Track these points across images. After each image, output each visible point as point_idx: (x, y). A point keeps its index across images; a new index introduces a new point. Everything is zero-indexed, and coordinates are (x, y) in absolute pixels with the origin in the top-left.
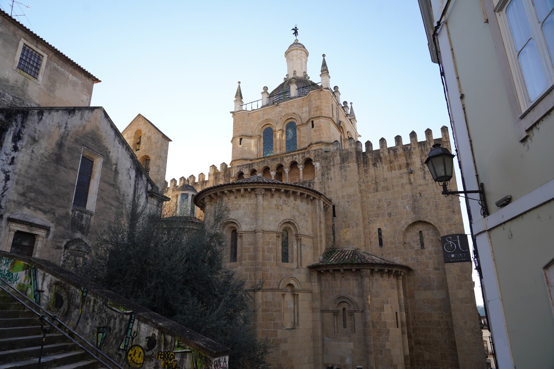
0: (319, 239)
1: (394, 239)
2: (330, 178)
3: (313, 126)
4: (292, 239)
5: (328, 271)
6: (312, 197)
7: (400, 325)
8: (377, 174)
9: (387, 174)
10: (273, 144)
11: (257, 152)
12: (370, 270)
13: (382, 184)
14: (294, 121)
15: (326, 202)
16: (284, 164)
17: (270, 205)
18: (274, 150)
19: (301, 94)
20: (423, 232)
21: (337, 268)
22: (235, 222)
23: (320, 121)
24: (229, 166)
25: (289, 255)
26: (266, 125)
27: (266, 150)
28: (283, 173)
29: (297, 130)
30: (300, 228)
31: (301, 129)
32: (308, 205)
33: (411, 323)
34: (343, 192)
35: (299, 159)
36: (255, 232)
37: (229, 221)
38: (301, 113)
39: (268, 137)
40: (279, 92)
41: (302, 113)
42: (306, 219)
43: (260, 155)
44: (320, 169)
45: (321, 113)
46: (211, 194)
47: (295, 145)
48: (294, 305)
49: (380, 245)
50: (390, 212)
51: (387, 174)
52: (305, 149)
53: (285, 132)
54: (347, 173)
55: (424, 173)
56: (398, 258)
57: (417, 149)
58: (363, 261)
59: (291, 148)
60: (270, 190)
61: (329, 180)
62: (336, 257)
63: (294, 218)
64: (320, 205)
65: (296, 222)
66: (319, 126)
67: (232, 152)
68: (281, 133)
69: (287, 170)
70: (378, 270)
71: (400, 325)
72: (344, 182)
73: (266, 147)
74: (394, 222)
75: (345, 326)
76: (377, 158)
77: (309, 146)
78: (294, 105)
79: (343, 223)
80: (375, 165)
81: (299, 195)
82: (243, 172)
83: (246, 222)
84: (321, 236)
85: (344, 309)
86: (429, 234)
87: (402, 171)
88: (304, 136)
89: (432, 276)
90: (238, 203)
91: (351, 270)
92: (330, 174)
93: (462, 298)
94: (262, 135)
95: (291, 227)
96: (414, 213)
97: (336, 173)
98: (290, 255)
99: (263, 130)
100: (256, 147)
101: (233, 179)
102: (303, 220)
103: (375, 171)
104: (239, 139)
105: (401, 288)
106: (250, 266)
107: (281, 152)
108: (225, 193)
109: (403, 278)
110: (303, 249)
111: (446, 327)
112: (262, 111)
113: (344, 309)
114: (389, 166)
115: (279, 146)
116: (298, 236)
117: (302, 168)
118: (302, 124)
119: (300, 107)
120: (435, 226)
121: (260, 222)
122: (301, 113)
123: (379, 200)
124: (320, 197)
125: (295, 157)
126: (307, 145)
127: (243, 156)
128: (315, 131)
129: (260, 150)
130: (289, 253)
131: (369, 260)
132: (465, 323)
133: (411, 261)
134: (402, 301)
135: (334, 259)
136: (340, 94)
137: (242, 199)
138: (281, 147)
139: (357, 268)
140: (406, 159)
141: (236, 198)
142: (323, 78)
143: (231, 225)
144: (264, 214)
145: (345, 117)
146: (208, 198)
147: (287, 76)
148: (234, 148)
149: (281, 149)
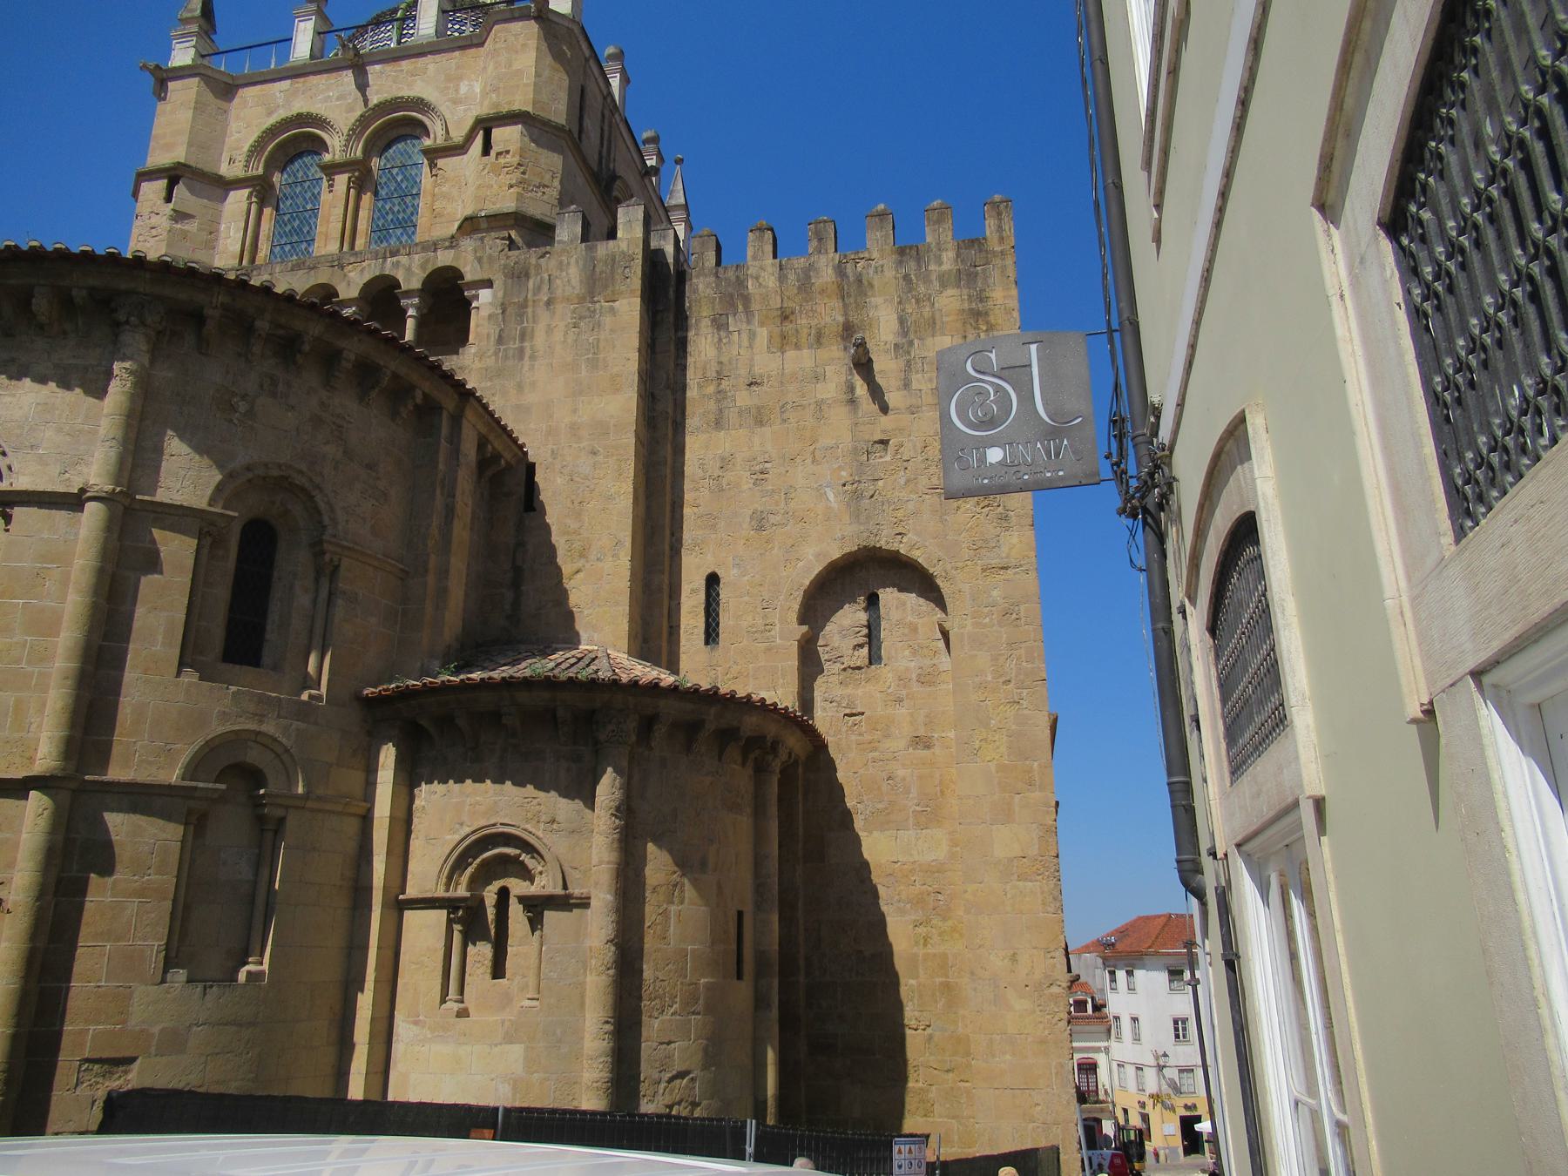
0: (431, 579)
2: (528, 352)
4: (293, 563)
7: (748, 967)
8: (724, 359)
9: (766, 362)
13: (744, 398)
15: (491, 438)
25: (268, 636)
33: (802, 963)
34: (575, 411)
35: (410, 273)
38: (449, 100)
44: (490, 316)
48: (257, 867)
49: (707, 643)
51: (766, 362)
54: (602, 337)
55: (908, 364)
57: (890, 273)
60: (196, 318)
61: (526, 358)
65: (318, 487)
66: (512, 148)
71: (748, 967)
72: (584, 373)
74: (772, 548)
75: (498, 970)
76: (731, 296)
80: (719, 324)
81: (349, 366)
83: (40, 451)
84: (444, 573)
85: (504, 894)
86: (904, 604)
87: (823, 354)
89: (901, 773)
90: (13, 360)
92: (532, 338)
93: (1011, 860)
96: (856, 515)
97: (558, 336)
98: (271, 635)
103: (719, 349)
104: (166, 181)
105: (773, 810)
106: (29, 662)
111: (938, 980)
113: (504, 894)
114: (777, 330)
123: (723, 459)
125: (395, 259)
127: (173, 252)
128: (496, 170)
130: (268, 628)
132: (1014, 958)
133: (824, 709)
134: (773, 866)
140: (845, 306)
145: (638, 178)
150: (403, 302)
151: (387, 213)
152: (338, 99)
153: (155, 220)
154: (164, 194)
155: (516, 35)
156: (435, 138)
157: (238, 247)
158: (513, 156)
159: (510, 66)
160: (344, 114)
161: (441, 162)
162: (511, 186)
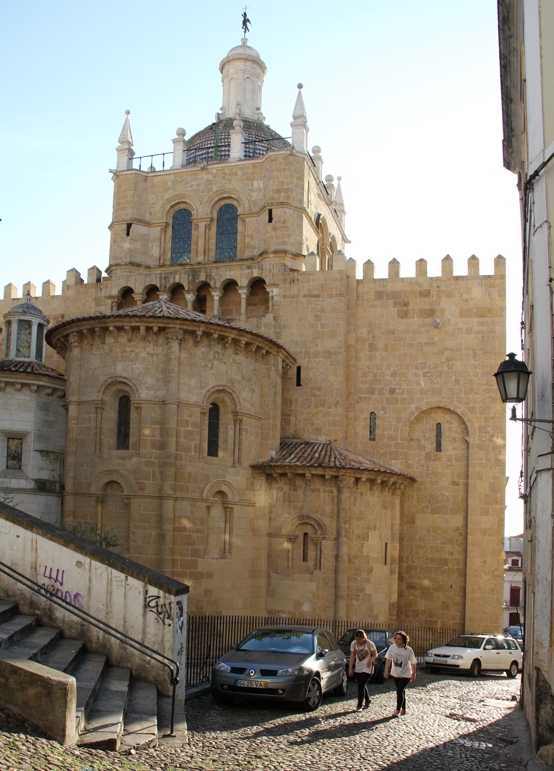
1: (394, 431)
3: (270, 220)
5: (284, 475)
6: (265, 350)
10: (191, 241)
11: (160, 253)
12: (354, 479)
14: (235, 203)
16: (212, 284)
17: (191, 358)
18: (193, 253)
19: (249, 152)
20: (442, 426)
21: (300, 472)
22: (128, 383)
23: (285, 212)
24: (104, 275)
26: (179, 203)
28: (208, 298)
29: (239, 222)
30: (242, 400)
31: (247, 220)
32: (257, 364)
36: (163, 403)
37: (116, 381)
38: (249, 190)
39: (181, 227)
40: (208, 140)
41: (252, 191)
42: (253, 387)
43: (164, 260)
45: (288, 197)
46: (82, 330)
47: (234, 249)
50: (393, 387)
52: (252, 259)
53: (215, 222)
56: (397, 461)
58: (343, 464)
59: (226, 253)
62: (298, 453)
63: (232, 383)
64: (278, 365)
67: (111, 247)
68: (209, 223)
69: (216, 295)
70: (367, 479)
77: (261, 255)
78: (236, 174)
79: (313, 399)
82: (133, 287)
88: (252, 235)
91: (323, 476)
94: (171, 221)
95: (227, 399)
99: (172, 212)
100: (159, 244)
101: (113, 300)
102: (246, 389)
107: (206, 258)
108: (109, 330)
109: (402, 493)
110: (243, 437)
115: (203, 247)
116: (238, 415)
117: (246, 293)
118: (251, 214)
119: (248, 179)
120: (463, 417)
121: (173, 386)
122: (249, 190)
124: (278, 352)
126: (256, 253)
128: (274, 229)
129: (164, 250)
131: (352, 462)
135: (295, 457)
136: (322, 163)
137: (141, 345)
139: (334, 474)
141: (130, 341)
142: (296, 131)
143: (120, 387)
144: (181, 373)
146: (75, 335)
147: (221, 109)
148: (114, 242)
149: (207, 254)
150: (240, 291)
151: (223, 241)
157: (158, 255)
158: (283, 223)
159: (278, 179)
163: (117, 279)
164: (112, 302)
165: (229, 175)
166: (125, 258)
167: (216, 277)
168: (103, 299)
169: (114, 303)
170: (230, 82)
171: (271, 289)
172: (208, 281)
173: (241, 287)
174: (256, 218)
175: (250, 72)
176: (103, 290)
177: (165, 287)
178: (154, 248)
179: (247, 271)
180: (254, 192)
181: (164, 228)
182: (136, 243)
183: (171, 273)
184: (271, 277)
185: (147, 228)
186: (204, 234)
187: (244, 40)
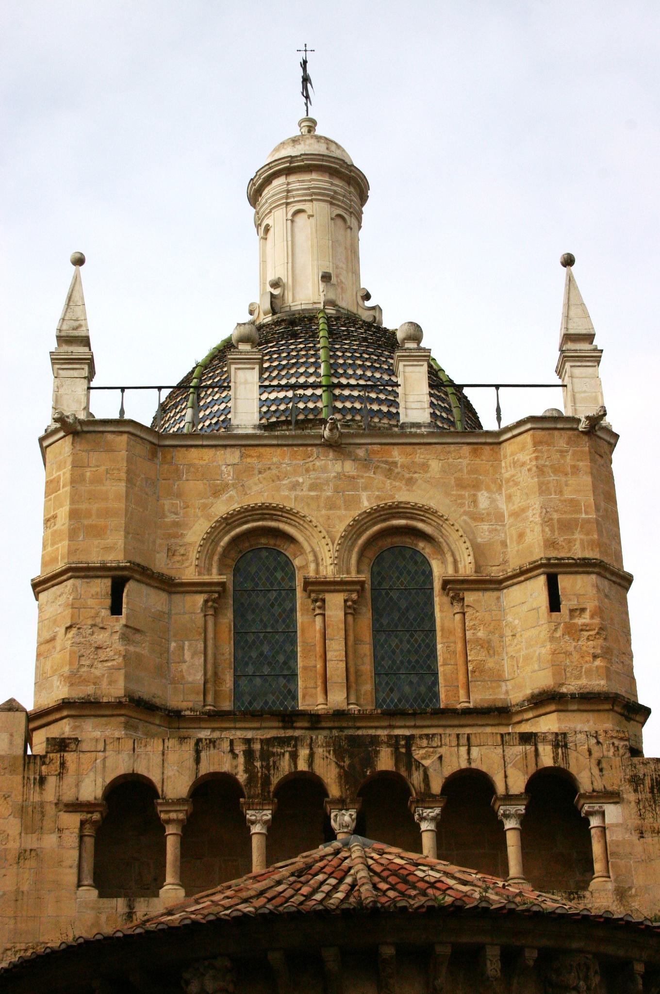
3: (554, 604)
10: (294, 643)
11: (205, 674)
27: (250, 670)
38: (465, 513)
41: (478, 518)
43: (217, 694)
53: (368, 594)
68: (354, 596)
73: (254, 654)
78: (425, 467)
82: (155, 778)
88: (489, 642)
100: (201, 646)
101: (85, 816)
104: (108, 582)
112: (237, 452)
115: (343, 665)
122: (465, 513)
129: (216, 666)
138: (352, 670)
152: (309, 490)
153: (101, 637)
154: (108, 602)
155: (561, 451)
156: (455, 562)
157: (199, 677)
159: (561, 492)
160: (324, 512)
161: (470, 597)
162: (595, 657)
163: (101, 747)
164: (83, 823)
165: (402, 466)
166: (111, 683)
167: (426, 763)
168: (50, 810)
169: (87, 826)
170: (292, 221)
171: (597, 807)
172: (403, 772)
173: (509, 798)
174: (495, 594)
175: (343, 202)
176: (52, 781)
177: (266, 781)
178: (187, 655)
179: (520, 748)
180: (482, 520)
181: (214, 601)
182: (138, 637)
183: (282, 741)
184: (596, 771)
185: (164, 596)
186: (342, 626)
187: (311, 125)
